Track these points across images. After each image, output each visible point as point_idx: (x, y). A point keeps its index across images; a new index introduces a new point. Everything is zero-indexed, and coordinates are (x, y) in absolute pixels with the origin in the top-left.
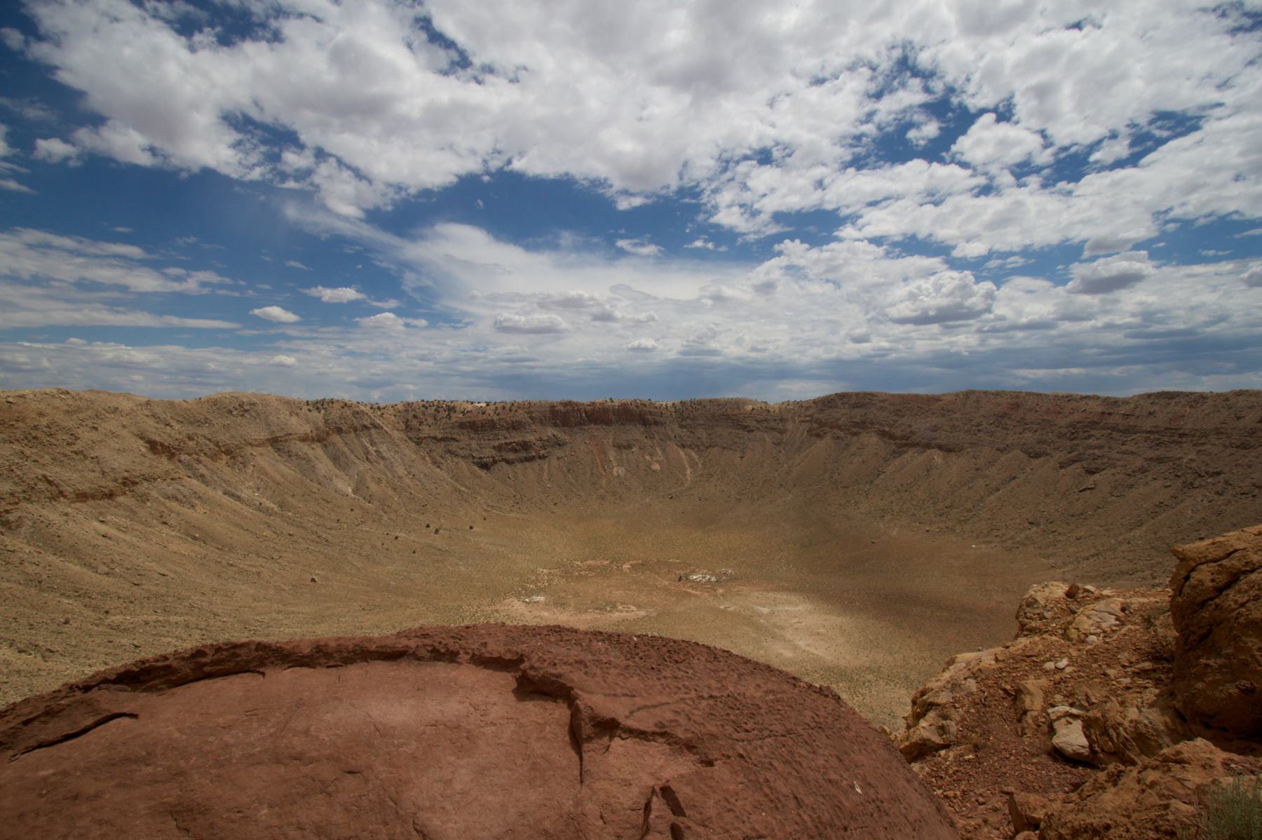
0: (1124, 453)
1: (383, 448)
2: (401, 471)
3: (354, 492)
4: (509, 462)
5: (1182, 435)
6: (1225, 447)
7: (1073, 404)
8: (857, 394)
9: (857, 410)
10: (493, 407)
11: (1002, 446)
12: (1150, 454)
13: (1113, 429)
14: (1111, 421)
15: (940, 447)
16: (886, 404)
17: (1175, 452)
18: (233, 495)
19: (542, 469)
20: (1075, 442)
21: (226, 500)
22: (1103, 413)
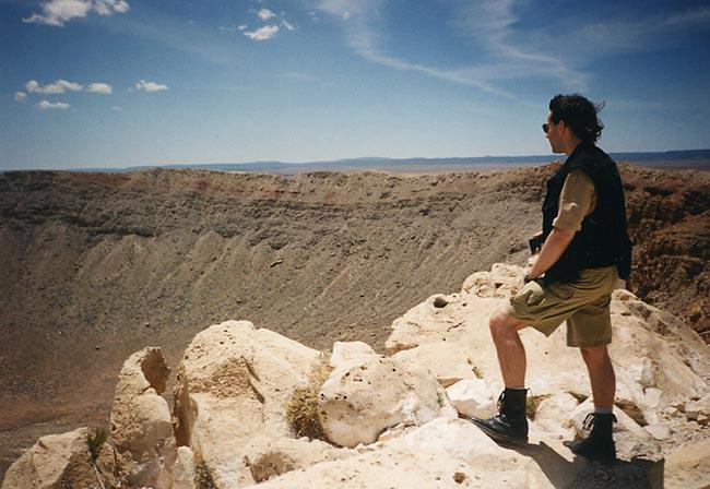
0: (299, 228)
5: (336, 210)
6: (364, 219)
7: (253, 183)
8: (33, 173)
9: (35, 193)
11: (197, 228)
12: (319, 227)
13: (287, 206)
14: (284, 198)
15: (138, 233)
16: (68, 185)
17: (332, 225)
20: (259, 220)
22: (277, 192)
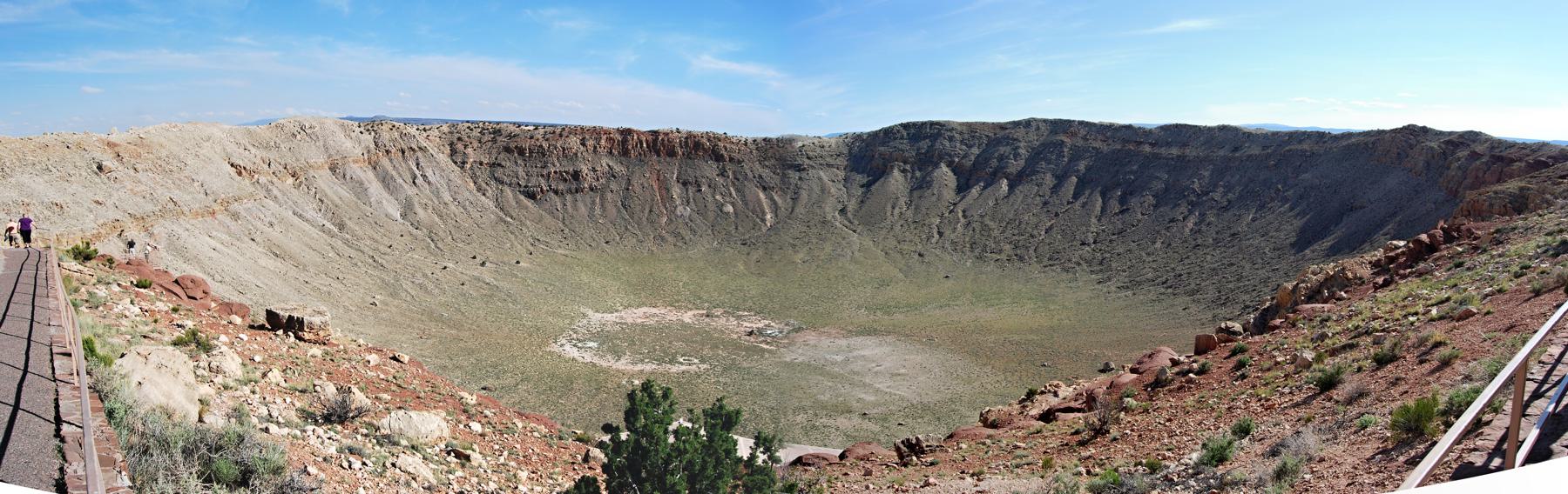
1: (429, 173)
2: (447, 197)
3: (404, 216)
4: (556, 192)
10: (541, 131)
18: (300, 216)
19: (593, 203)
21: (296, 220)
